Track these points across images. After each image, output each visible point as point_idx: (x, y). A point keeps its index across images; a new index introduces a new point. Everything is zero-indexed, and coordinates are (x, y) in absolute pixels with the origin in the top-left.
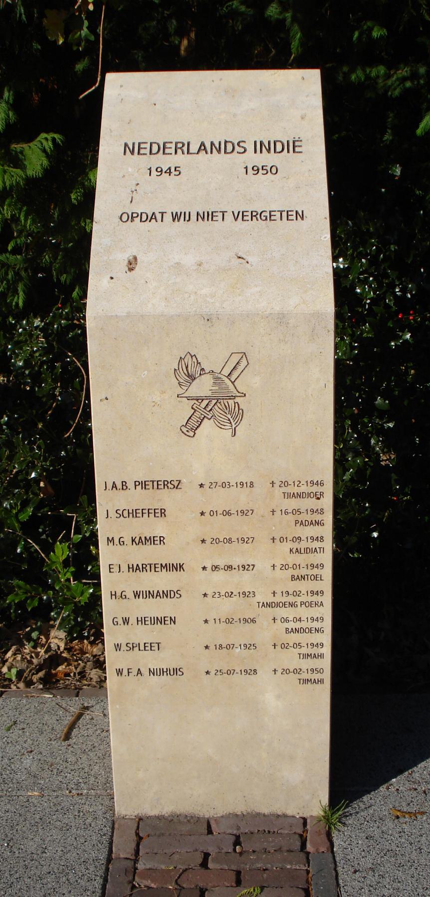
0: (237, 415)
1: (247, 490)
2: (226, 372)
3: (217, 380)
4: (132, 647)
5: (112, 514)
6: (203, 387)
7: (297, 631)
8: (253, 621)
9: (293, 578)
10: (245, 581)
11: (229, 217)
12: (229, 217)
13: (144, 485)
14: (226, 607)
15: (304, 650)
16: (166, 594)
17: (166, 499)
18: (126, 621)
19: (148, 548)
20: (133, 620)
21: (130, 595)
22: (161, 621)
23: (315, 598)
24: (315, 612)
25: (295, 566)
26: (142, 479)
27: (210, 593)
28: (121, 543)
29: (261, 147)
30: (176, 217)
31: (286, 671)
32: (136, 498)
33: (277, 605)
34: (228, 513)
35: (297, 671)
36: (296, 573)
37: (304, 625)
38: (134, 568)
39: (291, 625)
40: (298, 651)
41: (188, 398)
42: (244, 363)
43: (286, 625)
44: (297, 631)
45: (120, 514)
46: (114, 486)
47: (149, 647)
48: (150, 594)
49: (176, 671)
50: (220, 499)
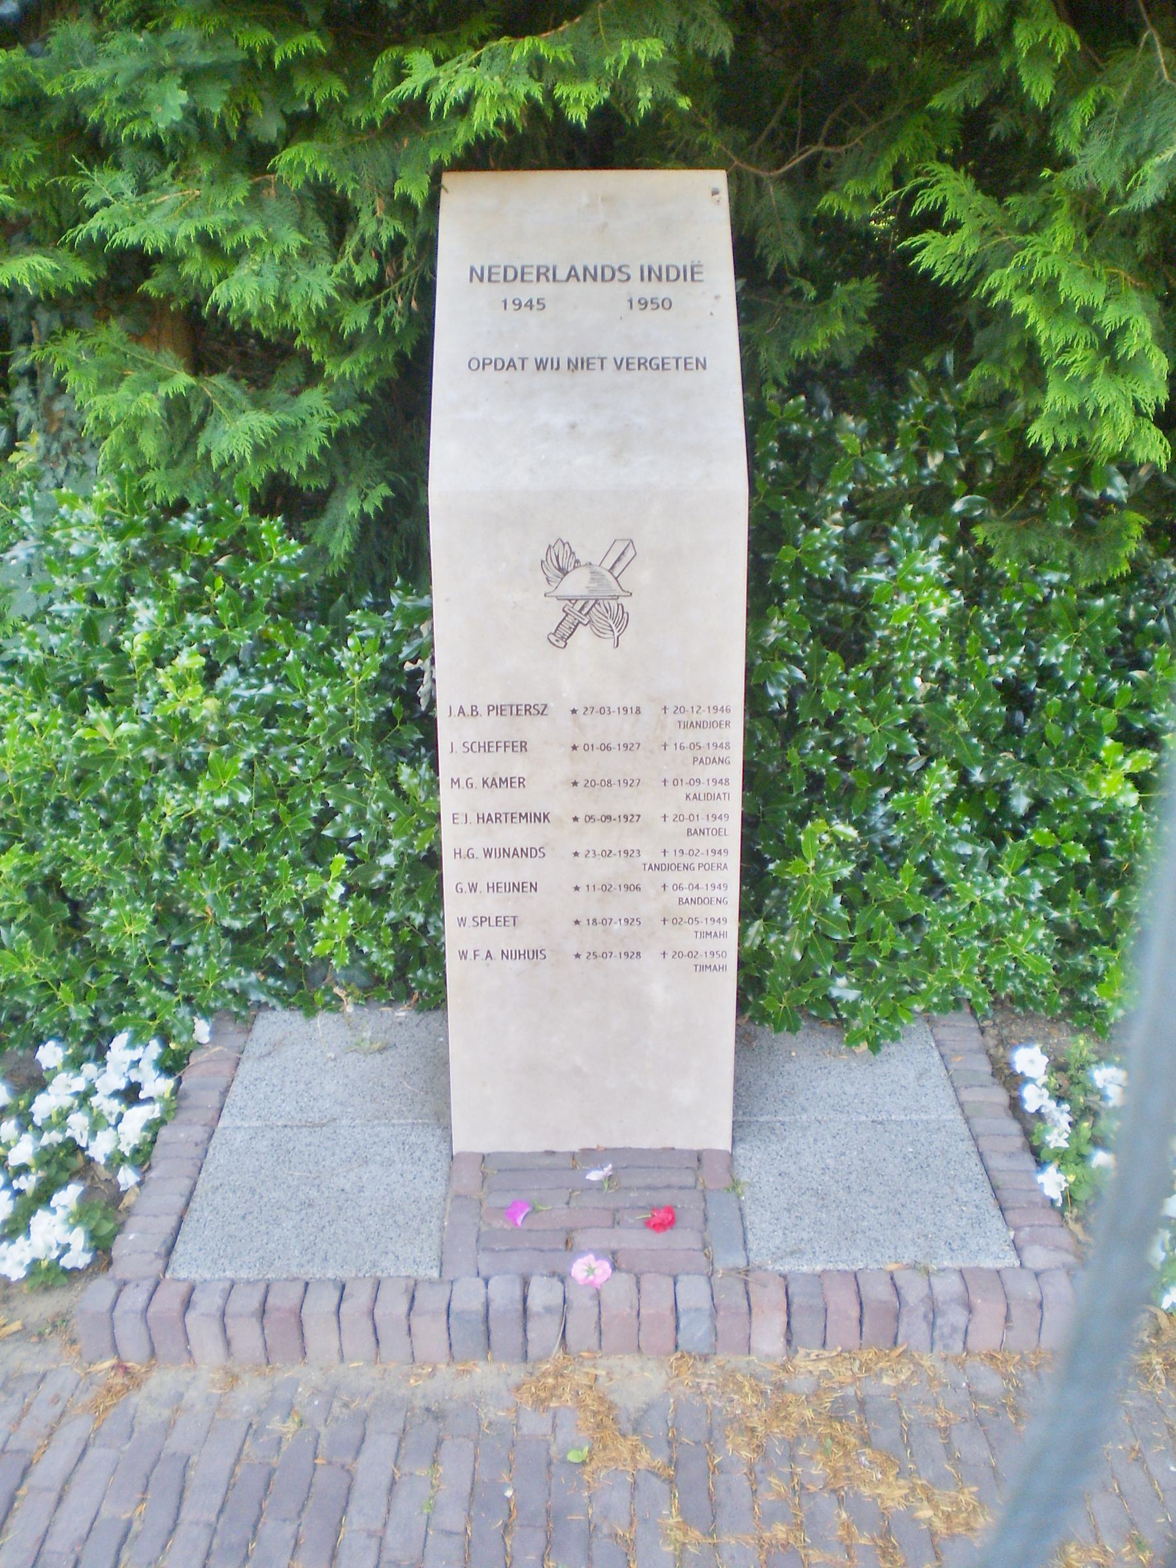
0: (621, 620)
1: (631, 718)
2: (608, 564)
3: (595, 576)
5: (458, 747)
6: (577, 584)
8: (637, 888)
11: (609, 365)
12: (609, 365)
13: (499, 710)
14: (600, 870)
15: (702, 927)
16: (525, 853)
17: (530, 729)
18: (473, 888)
19: (502, 792)
20: (482, 887)
21: (479, 853)
22: (518, 887)
26: (497, 700)
27: (582, 852)
29: (650, 274)
30: (541, 365)
31: (678, 954)
33: (669, 867)
35: (690, 954)
39: (686, 894)
40: (694, 927)
42: (630, 553)
43: (680, 894)
46: (461, 711)
50: (595, 730)
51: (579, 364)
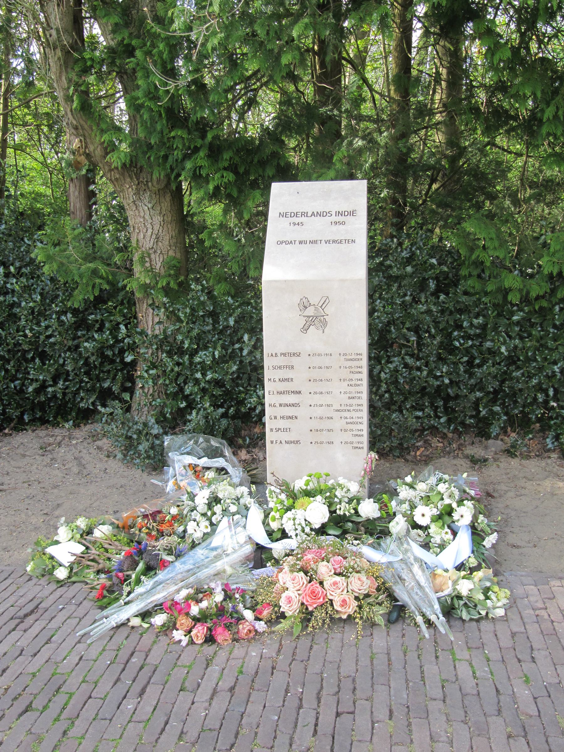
0: (324, 324)
1: (329, 357)
2: (320, 305)
3: (316, 309)
4: (278, 430)
5: (271, 368)
6: (310, 311)
7: (351, 423)
8: (332, 418)
9: (349, 398)
10: (327, 399)
12: (323, 242)
13: (284, 355)
14: (319, 412)
15: (355, 433)
16: (293, 405)
17: (294, 361)
18: (275, 418)
19: (286, 383)
20: (278, 417)
21: (278, 405)
22: (291, 418)
23: (359, 408)
24: (359, 414)
25: (350, 393)
26: (284, 352)
27: (313, 405)
28: (274, 381)
29: (338, 213)
30: (301, 242)
31: (346, 443)
32: (281, 361)
33: (342, 411)
34: (321, 368)
35: (352, 443)
36: (350, 395)
37: (354, 420)
38: (279, 393)
39: (349, 420)
40: (352, 433)
41: (304, 316)
42: (327, 301)
43: (346, 420)
44: (351, 423)
45: (274, 368)
46: (272, 355)
47: (285, 430)
48: (286, 405)
49: (297, 442)
50: (317, 361)
51: (315, 242)
